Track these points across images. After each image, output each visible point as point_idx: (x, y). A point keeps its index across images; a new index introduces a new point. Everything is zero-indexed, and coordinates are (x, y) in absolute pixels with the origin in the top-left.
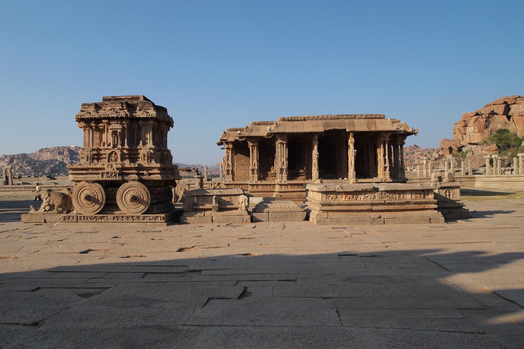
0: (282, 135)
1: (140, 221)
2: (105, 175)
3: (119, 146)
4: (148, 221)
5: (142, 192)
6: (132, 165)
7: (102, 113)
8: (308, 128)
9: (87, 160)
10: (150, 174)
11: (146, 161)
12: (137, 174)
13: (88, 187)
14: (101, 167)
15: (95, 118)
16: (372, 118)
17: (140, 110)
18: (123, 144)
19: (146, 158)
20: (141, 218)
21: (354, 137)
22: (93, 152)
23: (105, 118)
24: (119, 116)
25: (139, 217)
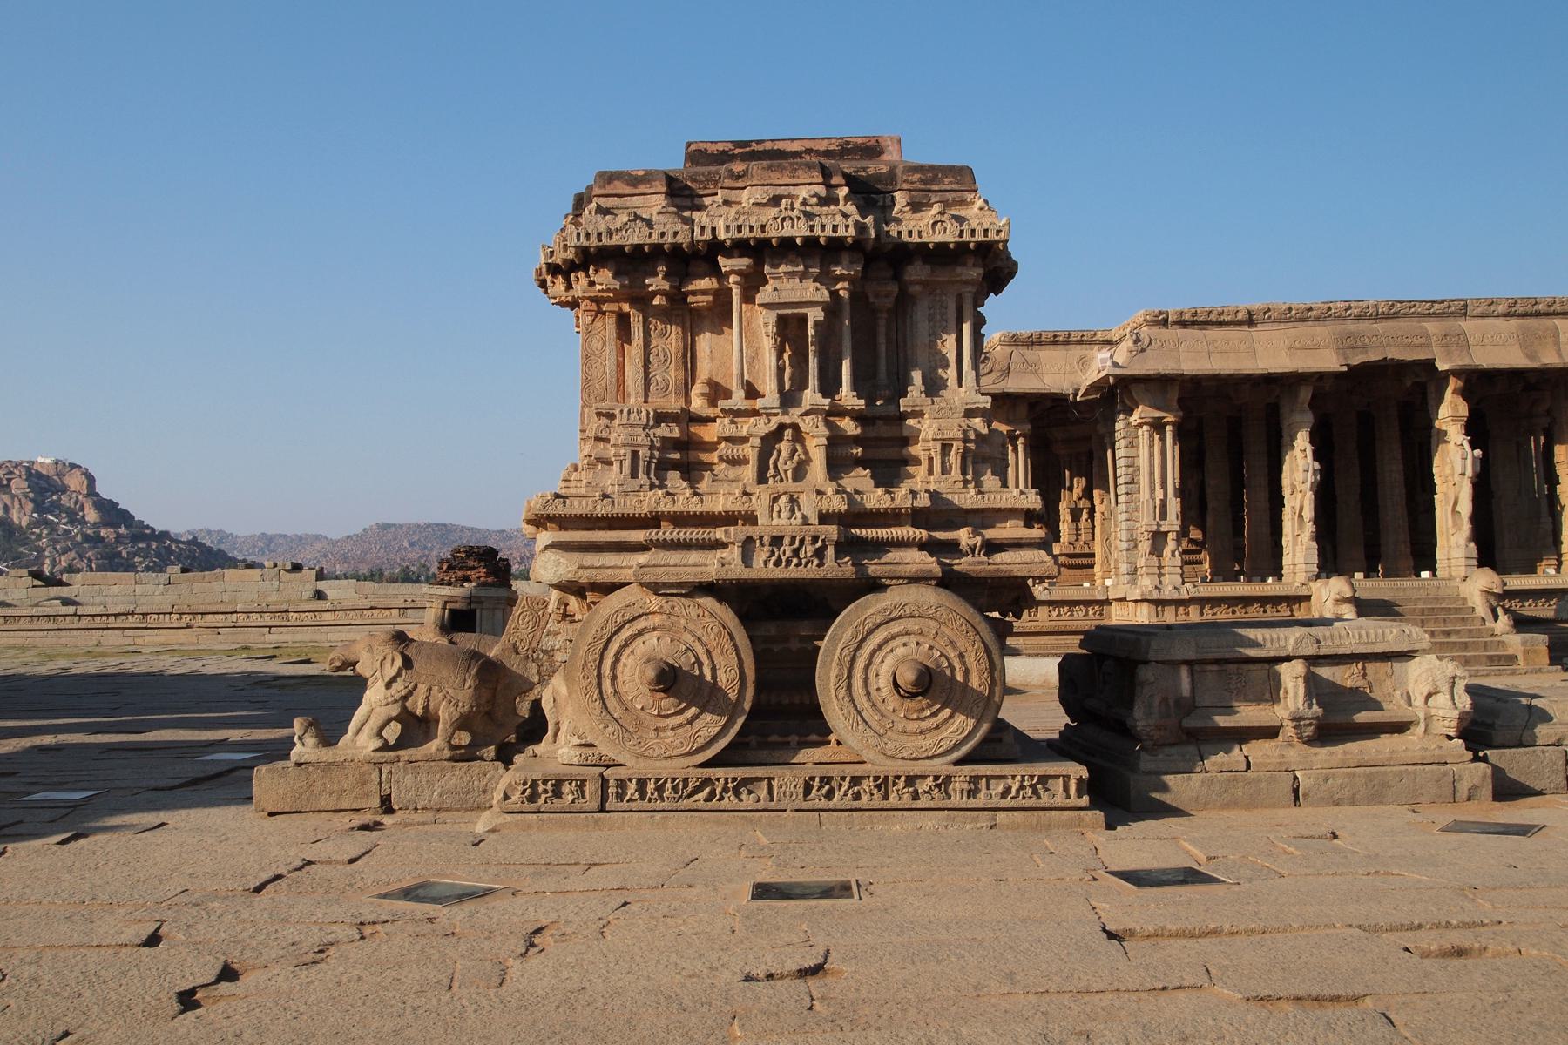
0: (1157, 386)
1: (956, 801)
2: (760, 556)
3: (811, 396)
4: (996, 802)
5: (962, 644)
6: (901, 497)
7: (717, 219)
8: (1270, 354)
9: (634, 474)
10: (992, 547)
11: (956, 473)
12: (923, 546)
13: (657, 620)
14: (739, 507)
15: (676, 248)
16: (1537, 314)
17: (916, 207)
18: (829, 386)
19: (954, 460)
20: (958, 785)
21: (1465, 393)
22: (663, 431)
23: (740, 247)
24: (823, 236)
25: (948, 779)
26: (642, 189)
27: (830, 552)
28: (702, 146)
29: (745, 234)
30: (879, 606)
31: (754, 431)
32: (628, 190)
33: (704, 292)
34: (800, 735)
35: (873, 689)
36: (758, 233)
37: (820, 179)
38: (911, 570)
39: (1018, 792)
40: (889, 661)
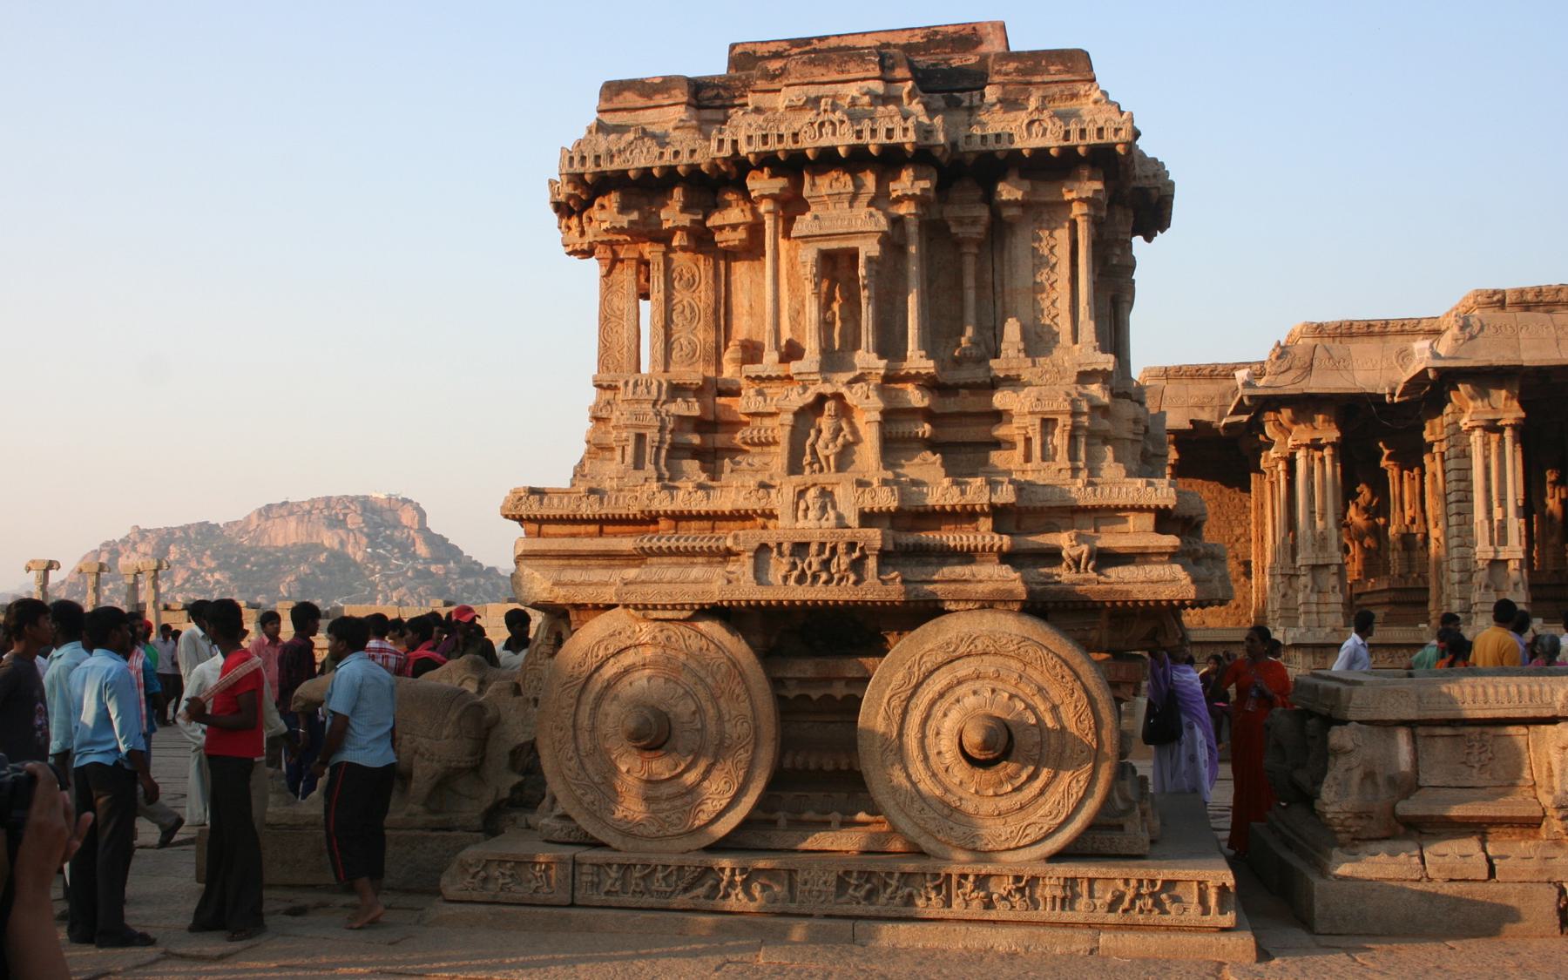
1: (1045, 912)
2: (778, 568)
3: (867, 358)
4: (1101, 915)
5: (1056, 693)
6: (976, 492)
7: (743, 132)
9: (638, 464)
10: (1105, 559)
11: (1062, 460)
12: (1006, 558)
14: (752, 504)
15: (694, 169)
17: (1010, 103)
18: (891, 345)
19: (1060, 440)
20: (1049, 889)
22: (679, 408)
23: (768, 161)
24: (873, 145)
25: (1034, 880)
26: (658, 99)
27: (872, 563)
28: (750, 48)
29: (773, 145)
30: (941, 639)
31: (785, 404)
33: (734, 227)
34: (844, 813)
35: (932, 752)
36: (788, 144)
37: (877, 73)
38: (983, 589)
39: (1132, 902)
40: (954, 715)
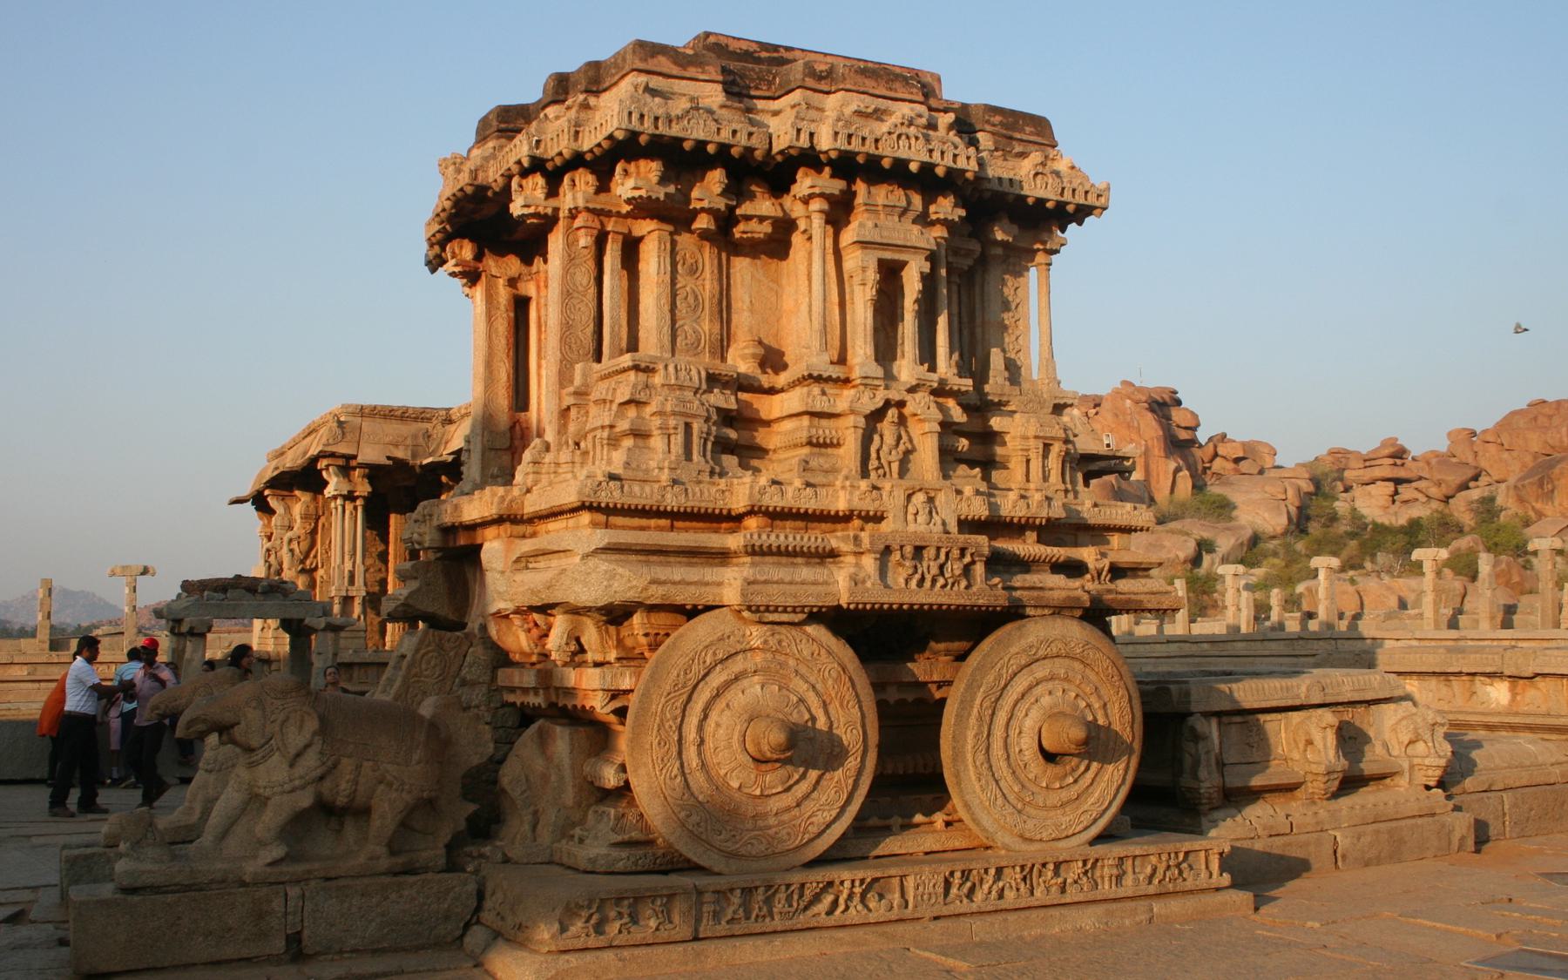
1: (1106, 889)
13: (759, 658)
20: (1107, 870)
26: (692, 72)
27: (979, 569)
28: (723, 41)
29: (855, 146)
30: (1024, 643)
31: (857, 406)
32: (675, 71)
33: (762, 219)
34: (903, 817)
35: (1014, 750)
36: (869, 148)
37: (921, 98)
38: (1057, 596)
40: (1034, 713)
